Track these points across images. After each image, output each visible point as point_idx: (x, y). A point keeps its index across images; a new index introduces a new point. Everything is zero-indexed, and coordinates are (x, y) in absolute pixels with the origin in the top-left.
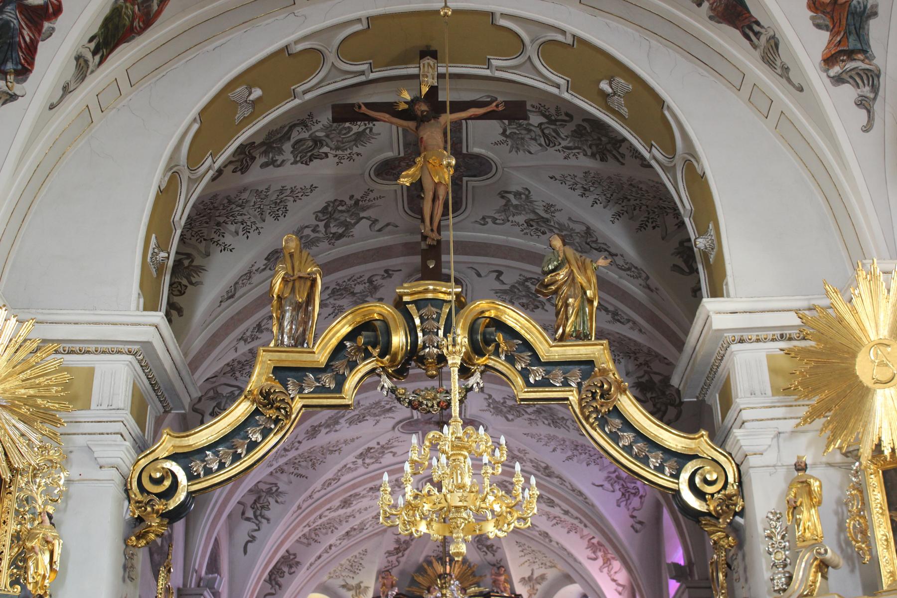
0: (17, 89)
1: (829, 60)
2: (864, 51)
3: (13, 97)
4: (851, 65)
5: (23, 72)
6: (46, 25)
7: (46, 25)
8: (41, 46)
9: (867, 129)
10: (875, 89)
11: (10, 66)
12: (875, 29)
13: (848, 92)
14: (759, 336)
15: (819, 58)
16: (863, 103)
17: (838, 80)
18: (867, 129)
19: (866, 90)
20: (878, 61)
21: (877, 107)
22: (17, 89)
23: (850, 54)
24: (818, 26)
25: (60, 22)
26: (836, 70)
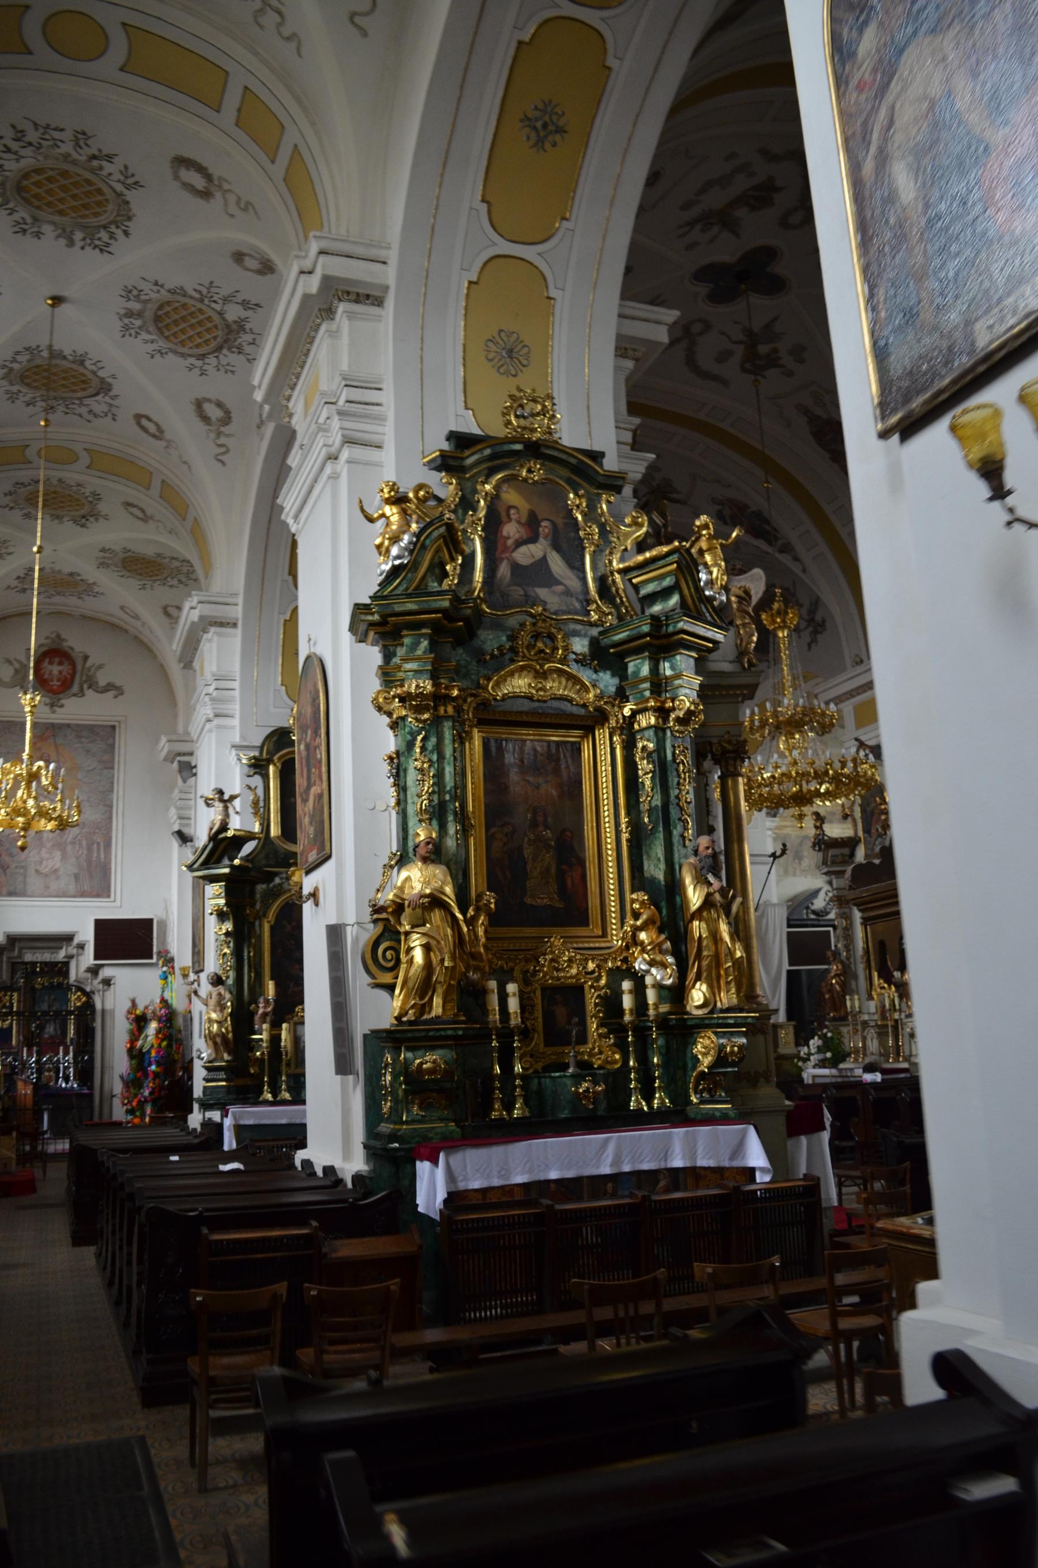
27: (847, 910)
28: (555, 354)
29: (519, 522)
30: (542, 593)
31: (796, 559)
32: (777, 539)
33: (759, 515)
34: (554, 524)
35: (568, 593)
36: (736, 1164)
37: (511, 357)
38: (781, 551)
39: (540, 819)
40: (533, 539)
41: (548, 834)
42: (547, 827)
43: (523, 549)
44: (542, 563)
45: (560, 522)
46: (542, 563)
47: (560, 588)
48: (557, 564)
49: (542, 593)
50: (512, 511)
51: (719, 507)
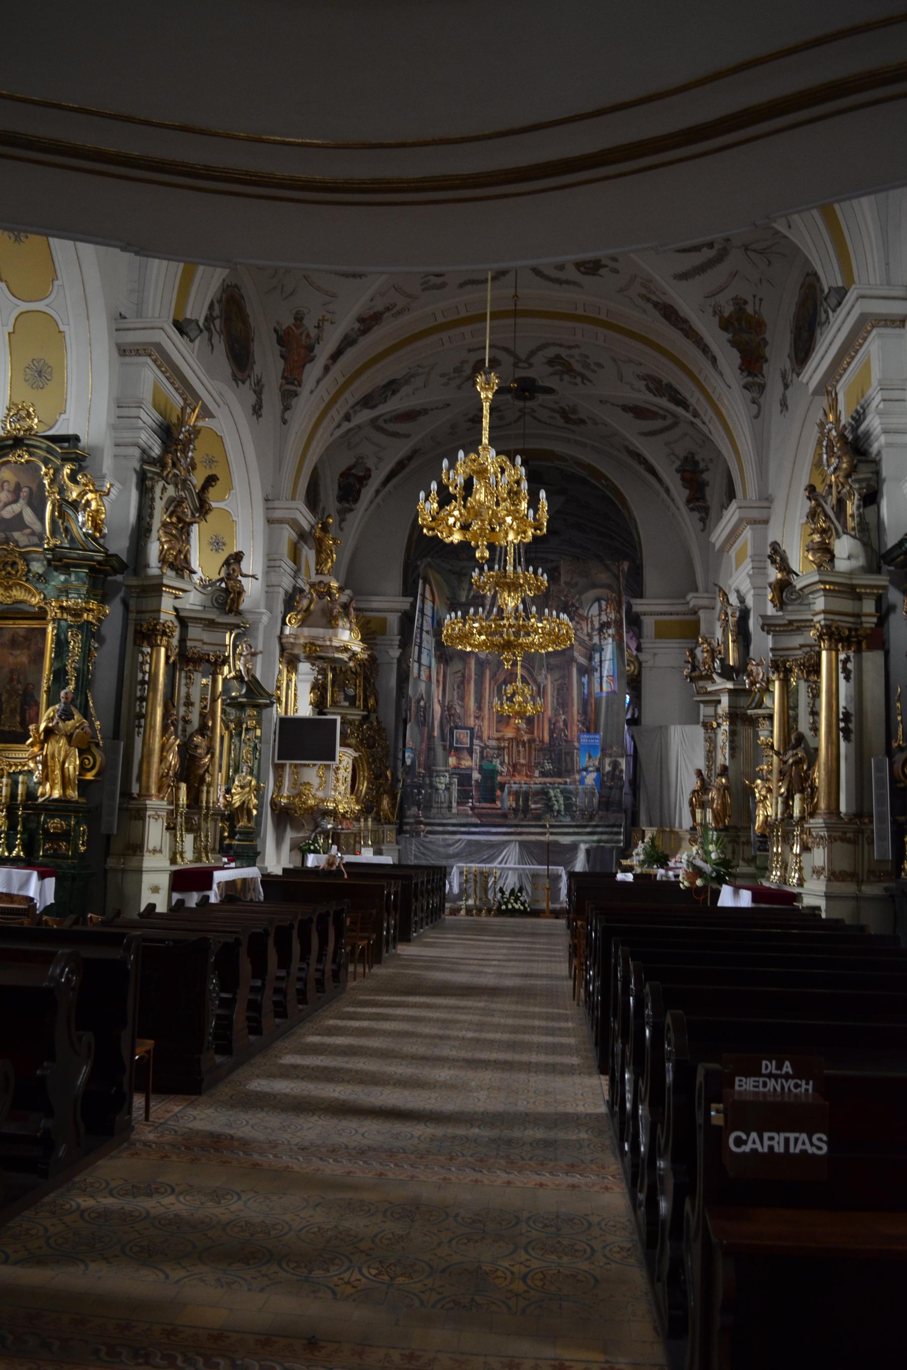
0: (354, 507)
1: (689, 501)
2: (703, 498)
3: (351, 510)
4: (698, 504)
5: (356, 500)
6: (365, 482)
7: (365, 482)
8: (364, 491)
9: (703, 530)
10: (707, 514)
11: (351, 498)
12: (708, 491)
13: (696, 515)
14: (651, 614)
15: (684, 500)
16: (703, 520)
17: (692, 510)
18: (703, 530)
19: (704, 515)
20: (709, 503)
21: (707, 522)
22: (354, 507)
23: (698, 500)
24: (685, 487)
25: (370, 481)
26: (692, 505)
27: (712, 735)
28: (69, 369)
29: (9, 491)
30: (17, 535)
31: (704, 423)
32: (688, 406)
33: (669, 386)
34: (30, 489)
35: (33, 533)
36: (22, 893)
37: (40, 376)
38: (695, 417)
39: (15, 677)
40: (15, 501)
41: (19, 686)
42: (19, 682)
43: (9, 508)
44: (20, 515)
45: (34, 487)
46: (20, 515)
47: (28, 531)
48: (29, 516)
49: (17, 535)
50: (5, 484)
51: (645, 382)
